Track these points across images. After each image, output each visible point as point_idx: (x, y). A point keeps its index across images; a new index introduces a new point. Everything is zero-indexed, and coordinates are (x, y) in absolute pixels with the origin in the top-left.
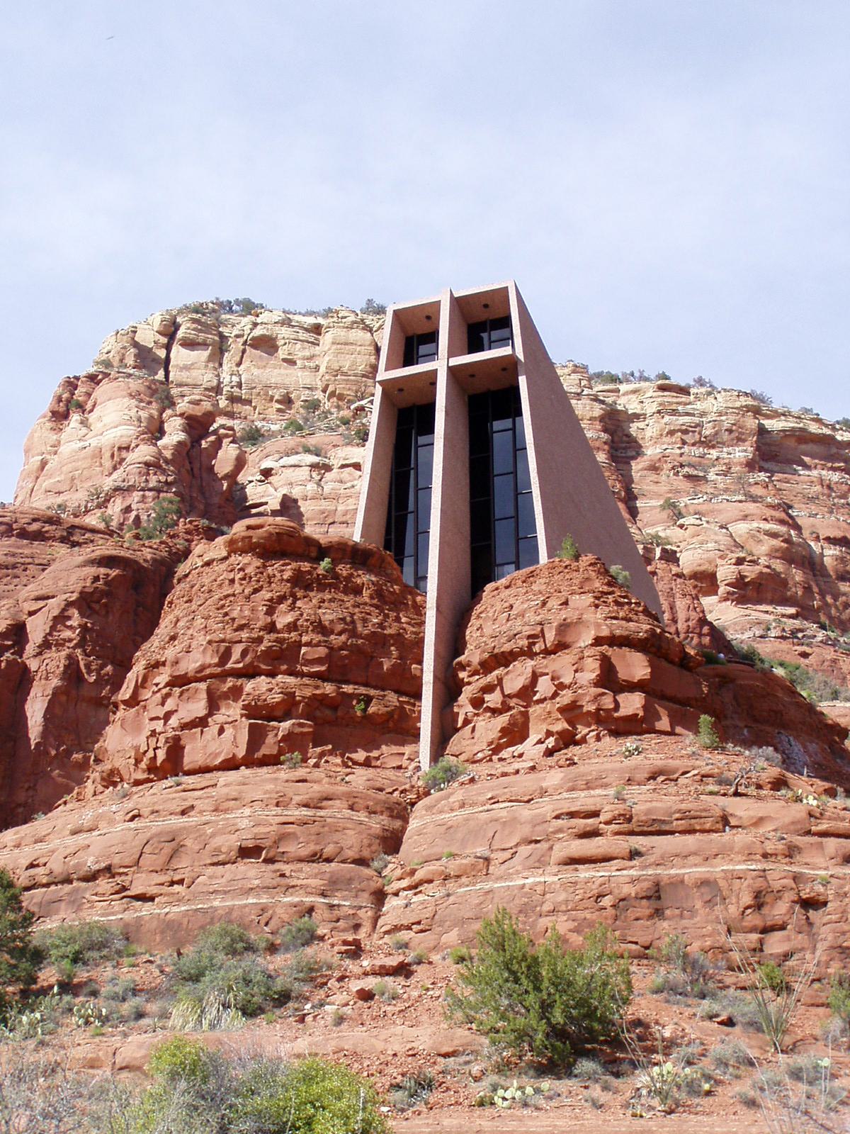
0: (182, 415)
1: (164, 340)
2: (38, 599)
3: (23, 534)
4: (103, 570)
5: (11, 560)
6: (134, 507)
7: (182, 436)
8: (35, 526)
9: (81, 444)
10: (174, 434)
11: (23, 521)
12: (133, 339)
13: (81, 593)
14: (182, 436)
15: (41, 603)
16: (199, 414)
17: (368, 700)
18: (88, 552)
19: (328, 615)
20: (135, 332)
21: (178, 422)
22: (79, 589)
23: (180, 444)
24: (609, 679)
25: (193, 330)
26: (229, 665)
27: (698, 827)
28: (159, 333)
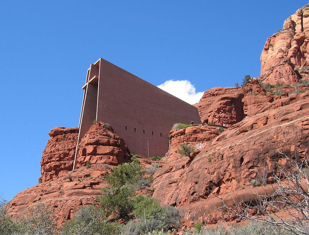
0: (295, 40)
1: (300, 17)
2: (210, 112)
3: (213, 95)
4: (222, 101)
5: (210, 103)
6: (278, 70)
7: (296, 46)
8: (216, 92)
9: (271, 56)
10: (294, 45)
11: (213, 92)
12: (291, 20)
13: (218, 109)
14: (296, 46)
15: (211, 113)
16: (299, 38)
17: (65, 164)
18: (220, 97)
19: (60, 147)
20: (291, 18)
21: (295, 42)
22: (217, 108)
23: (295, 48)
24: (84, 153)
25: (307, 12)
26: (44, 162)
27: (54, 191)
28: (298, 16)
